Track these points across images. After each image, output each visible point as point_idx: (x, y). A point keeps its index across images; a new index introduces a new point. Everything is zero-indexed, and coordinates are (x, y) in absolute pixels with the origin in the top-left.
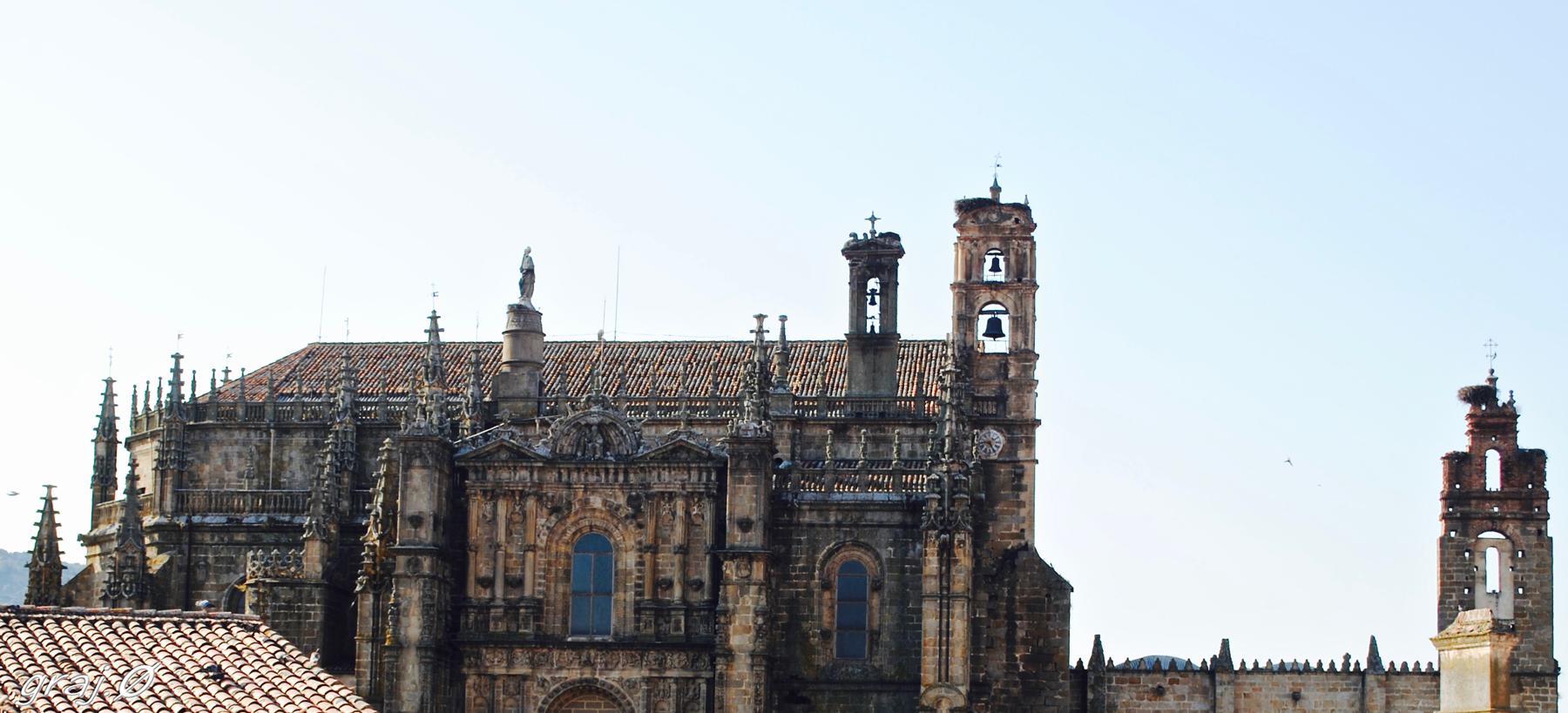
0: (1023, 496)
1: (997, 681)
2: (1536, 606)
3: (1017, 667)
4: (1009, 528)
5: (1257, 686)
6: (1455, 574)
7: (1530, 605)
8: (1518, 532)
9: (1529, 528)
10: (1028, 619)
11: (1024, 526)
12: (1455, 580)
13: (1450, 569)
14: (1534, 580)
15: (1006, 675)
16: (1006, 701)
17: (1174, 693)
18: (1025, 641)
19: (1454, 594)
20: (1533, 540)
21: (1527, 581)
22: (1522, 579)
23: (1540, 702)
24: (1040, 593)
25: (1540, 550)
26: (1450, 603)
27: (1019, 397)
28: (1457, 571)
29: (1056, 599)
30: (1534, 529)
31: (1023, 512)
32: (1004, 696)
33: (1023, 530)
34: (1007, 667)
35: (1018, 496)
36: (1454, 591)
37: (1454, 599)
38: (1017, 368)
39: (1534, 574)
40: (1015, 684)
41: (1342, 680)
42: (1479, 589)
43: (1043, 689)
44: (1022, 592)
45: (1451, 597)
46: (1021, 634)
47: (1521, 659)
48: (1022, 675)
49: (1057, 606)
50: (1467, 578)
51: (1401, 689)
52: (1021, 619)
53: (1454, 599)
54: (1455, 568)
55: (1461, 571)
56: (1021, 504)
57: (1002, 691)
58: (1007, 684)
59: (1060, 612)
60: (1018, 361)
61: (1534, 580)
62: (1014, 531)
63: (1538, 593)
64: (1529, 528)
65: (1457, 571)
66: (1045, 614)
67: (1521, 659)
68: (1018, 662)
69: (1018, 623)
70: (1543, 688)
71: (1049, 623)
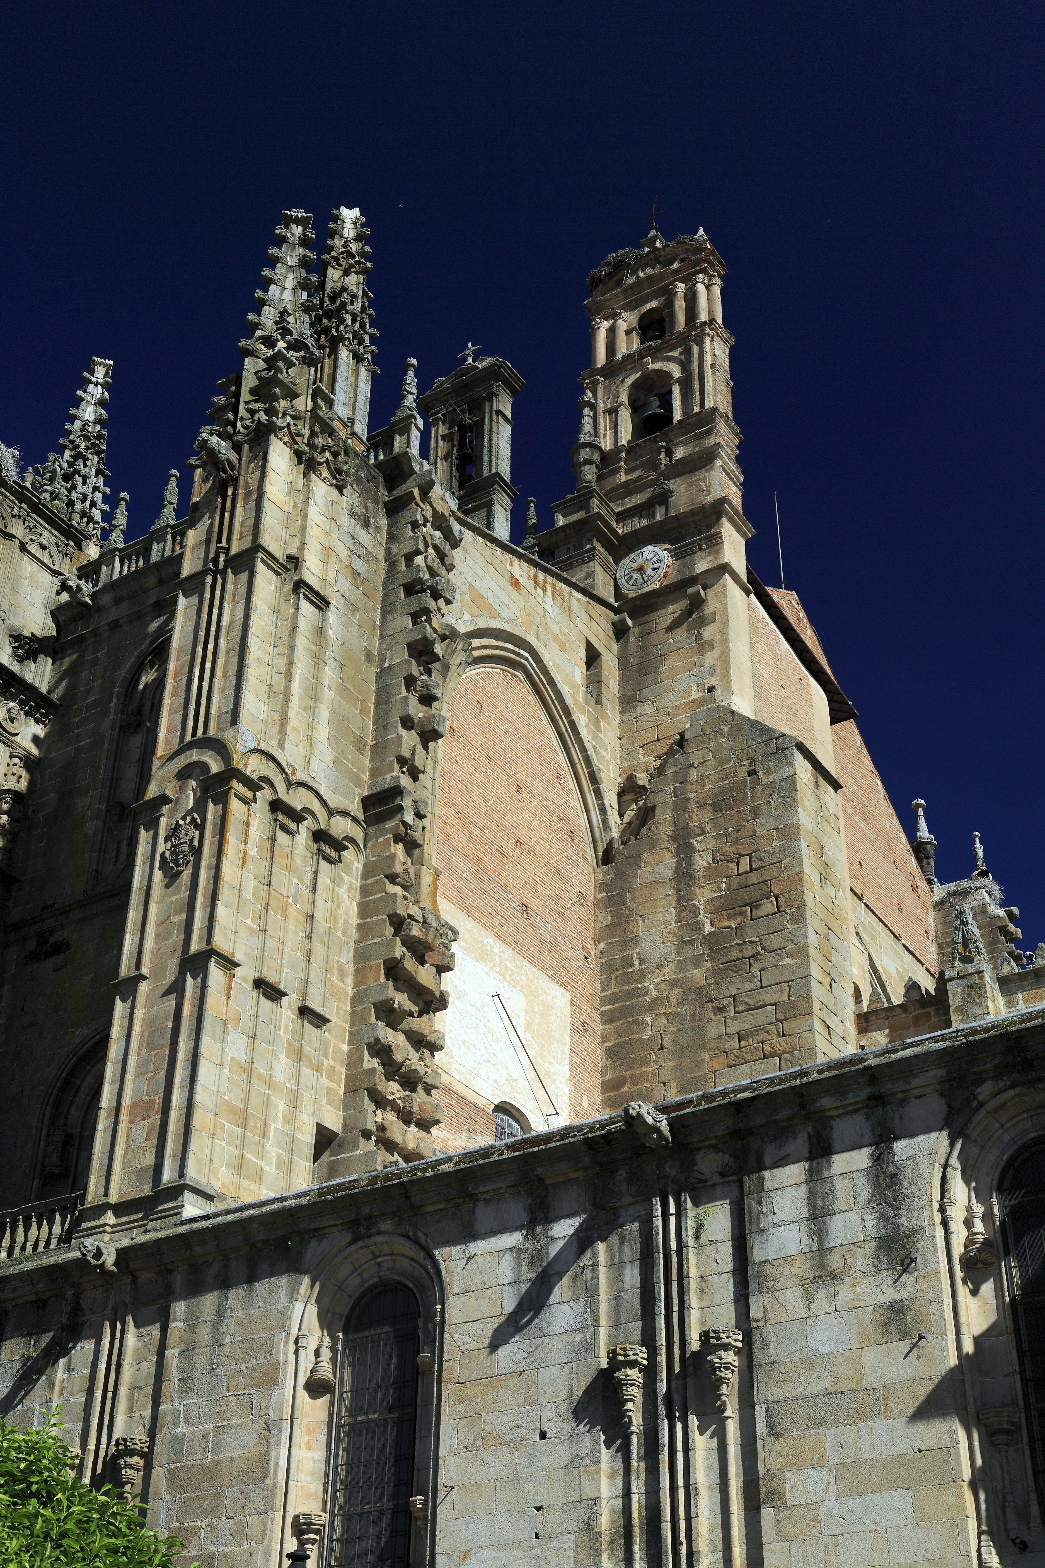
0: (708, 633)
1: (661, 966)
3: (699, 927)
18: (712, 873)
27: (691, 485)
29: (768, 773)
31: (711, 658)
32: (677, 991)
40: (697, 962)
46: (701, 862)
48: (714, 942)
56: (704, 647)
57: (672, 984)
58: (680, 966)
62: (695, 695)
68: (701, 916)
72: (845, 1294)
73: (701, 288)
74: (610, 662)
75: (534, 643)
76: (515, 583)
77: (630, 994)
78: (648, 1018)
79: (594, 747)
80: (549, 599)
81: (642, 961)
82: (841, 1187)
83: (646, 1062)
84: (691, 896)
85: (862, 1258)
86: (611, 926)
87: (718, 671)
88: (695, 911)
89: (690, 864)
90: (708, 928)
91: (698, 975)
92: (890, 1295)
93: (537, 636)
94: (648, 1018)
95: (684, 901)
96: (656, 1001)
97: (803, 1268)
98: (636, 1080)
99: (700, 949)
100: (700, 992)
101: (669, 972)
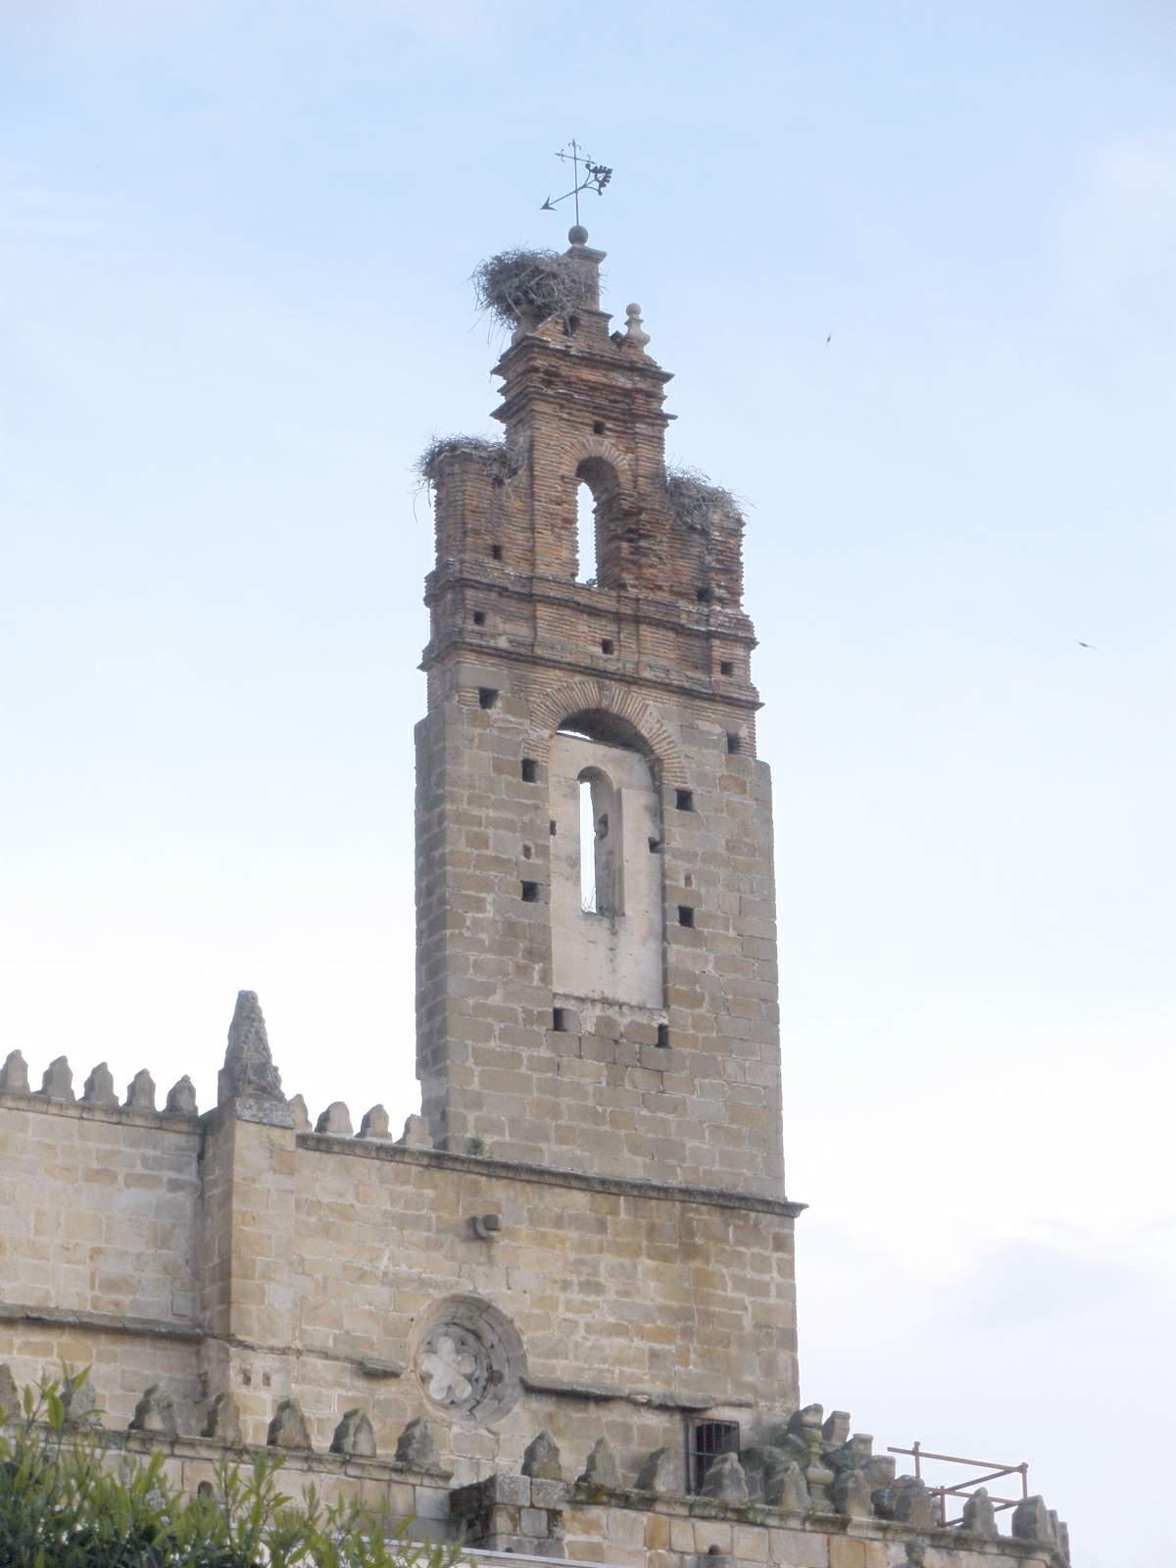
2: (731, 976)
6: (490, 832)
7: (710, 968)
8: (671, 729)
9: (704, 725)
12: (489, 852)
13: (475, 812)
14: (720, 888)
19: (489, 898)
20: (714, 760)
21: (703, 891)
22: (688, 880)
23: (748, 1299)
25: (736, 798)
26: (477, 925)
28: (496, 824)
30: (717, 730)
36: (487, 885)
37: (489, 913)
39: (722, 873)
41: (133, 1144)
42: (557, 890)
45: (479, 905)
47: (691, 1143)
50: (527, 851)
51: (326, 1200)
53: (489, 913)
54: (492, 814)
55: (510, 825)
61: (720, 888)
63: (732, 933)
64: (704, 725)
65: (496, 824)
67: (691, 1143)
70: (756, 1250)
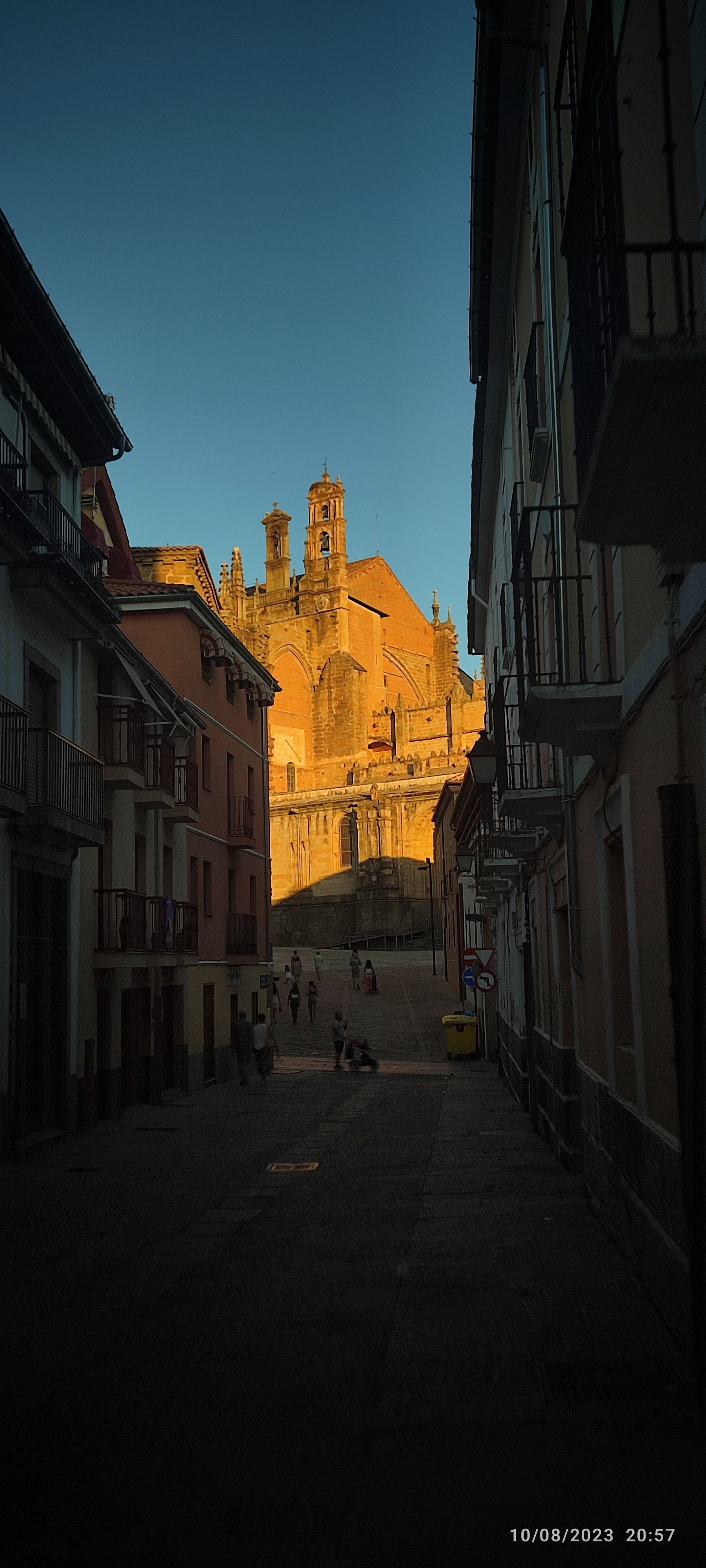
0: (337, 626)
1: (325, 721)
3: (333, 712)
4: (332, 644)
5: (475, 708)
10: (336, 687)
11: (338, 641)
15: (329, 717)
16: (329, 730)
17: (438, 718)
18: (336, 699)
24: (340, 674)
31: (337, 635)
32: (328, 728)
33: (337, 644)
34: (328, 713)
35: (335, 627)
38: (332, 563)
40: (332, 721)
43: (343, 721)
44: (333, 674)
46: (334, 695)
48: (335, 716)
49: (348, 678)
52: (333, 688)
57: (328, 725)
58: (329, 721)
59: (349, 681)
60: (332, 559)
62: (334, 645)
66: (343, 684)
69: (332, 690)
71: (345, 688)
72: (320, 836)
73: (337, 504)
74: (314, 631)
75: (292, 642)
76: (286, 630)
77: (319, 726)
78: (322, 733)
79: (310, 661)
80: (295, 626)
81: (321, 719)
82: (320, 823)
83: (322, 743)
84: (331, 704)
85: (322, 832)
86: (315, 708)
87: (339, 639)
88: (332, 708)
89: (331, 695)
90: (335, 713)
91: (333, 724)
92: (325, 838)
93: (293, 641)
94: (322, 733)
95: (330, 704)
96: (323, 730)
97: (315, 833)
98: (321, 747)
99: (333, 718)
100: (333, 729)
101: (326, 723)
